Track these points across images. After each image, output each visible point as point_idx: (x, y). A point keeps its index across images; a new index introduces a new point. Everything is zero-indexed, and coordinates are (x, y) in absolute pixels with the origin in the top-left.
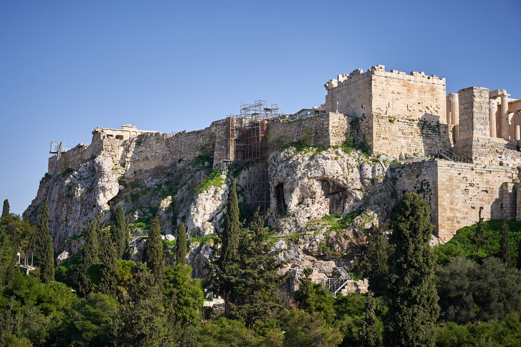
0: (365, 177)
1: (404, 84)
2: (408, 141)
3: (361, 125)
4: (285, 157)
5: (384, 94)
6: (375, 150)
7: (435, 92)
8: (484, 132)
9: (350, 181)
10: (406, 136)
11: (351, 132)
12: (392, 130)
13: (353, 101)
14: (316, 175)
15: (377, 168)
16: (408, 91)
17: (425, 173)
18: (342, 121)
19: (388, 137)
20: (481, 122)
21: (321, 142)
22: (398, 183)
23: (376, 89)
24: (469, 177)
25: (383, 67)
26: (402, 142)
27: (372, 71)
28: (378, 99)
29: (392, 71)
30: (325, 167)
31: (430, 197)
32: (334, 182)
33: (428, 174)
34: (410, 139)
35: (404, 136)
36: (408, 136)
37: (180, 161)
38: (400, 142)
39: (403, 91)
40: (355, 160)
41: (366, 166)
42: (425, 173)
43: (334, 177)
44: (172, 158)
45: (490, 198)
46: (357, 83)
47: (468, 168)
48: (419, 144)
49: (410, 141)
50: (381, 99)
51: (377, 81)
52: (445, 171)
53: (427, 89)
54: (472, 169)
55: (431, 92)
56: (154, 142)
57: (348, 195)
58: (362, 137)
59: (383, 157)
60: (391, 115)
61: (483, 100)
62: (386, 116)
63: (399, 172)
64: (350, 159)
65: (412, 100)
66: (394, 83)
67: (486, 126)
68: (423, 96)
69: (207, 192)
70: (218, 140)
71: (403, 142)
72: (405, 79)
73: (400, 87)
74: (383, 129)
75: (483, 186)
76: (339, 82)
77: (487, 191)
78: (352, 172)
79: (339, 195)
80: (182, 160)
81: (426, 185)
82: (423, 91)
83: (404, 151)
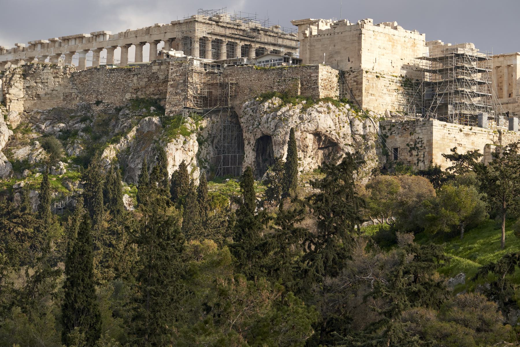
0: (356, 133)
3: (348, 79)
4: (269, 108)
6: (364, 106)
7: (416, 48)
9: (343, 136)
12: (379, 86)
13: (338, 53)
14: (309, 128)
15: (368, 123)
16: (393, 46)
17: (420, 131)
18: (330, 74)
19: (375, 94)
21: (309, 94)
22: (388, 141)
24: (458, 137)
25: (372, 20)
27: (361, 25)
29: (378, 25)
30: (319, 121)
31: (424, 155)
32: (326, 136)
33: (422, 132)
34: (394, 96)
35: (389, 93)
37: (98, 103)
41: (357, 122)
42: (420, 131)
43: (327, 131)
44: (81, 99)
46: (343, 35)
47: (457, 128)
49: (394, 98)
54: (461, 131)
56: (51, 77)
57: (339, 150)
58: (349, 92)
59: (371, 113)
60: (378, 71)
62: (373, 71)
63: (390, 130)
64: (341, 113)
69: (177, 141)
70: (172, 82)
72: (391, 34)
74: (371, 85)
76: (319, 31)
78: (344, 127)
79: (329, 150)
80: (101, 102)
81: (420, 143)
82: (405, 46)
83: (389, 109)
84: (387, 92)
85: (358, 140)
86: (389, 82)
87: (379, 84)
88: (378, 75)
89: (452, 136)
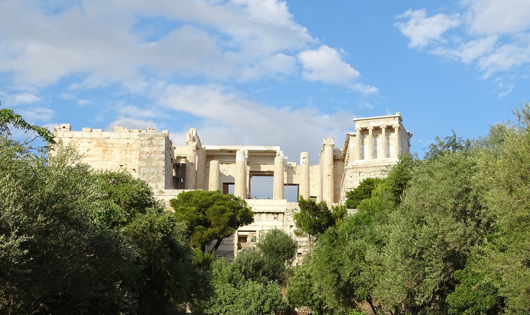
1: (99, 143)
16: (104, 152)
61: (154, 149)
67: (158, 184)
68: (128, 156)
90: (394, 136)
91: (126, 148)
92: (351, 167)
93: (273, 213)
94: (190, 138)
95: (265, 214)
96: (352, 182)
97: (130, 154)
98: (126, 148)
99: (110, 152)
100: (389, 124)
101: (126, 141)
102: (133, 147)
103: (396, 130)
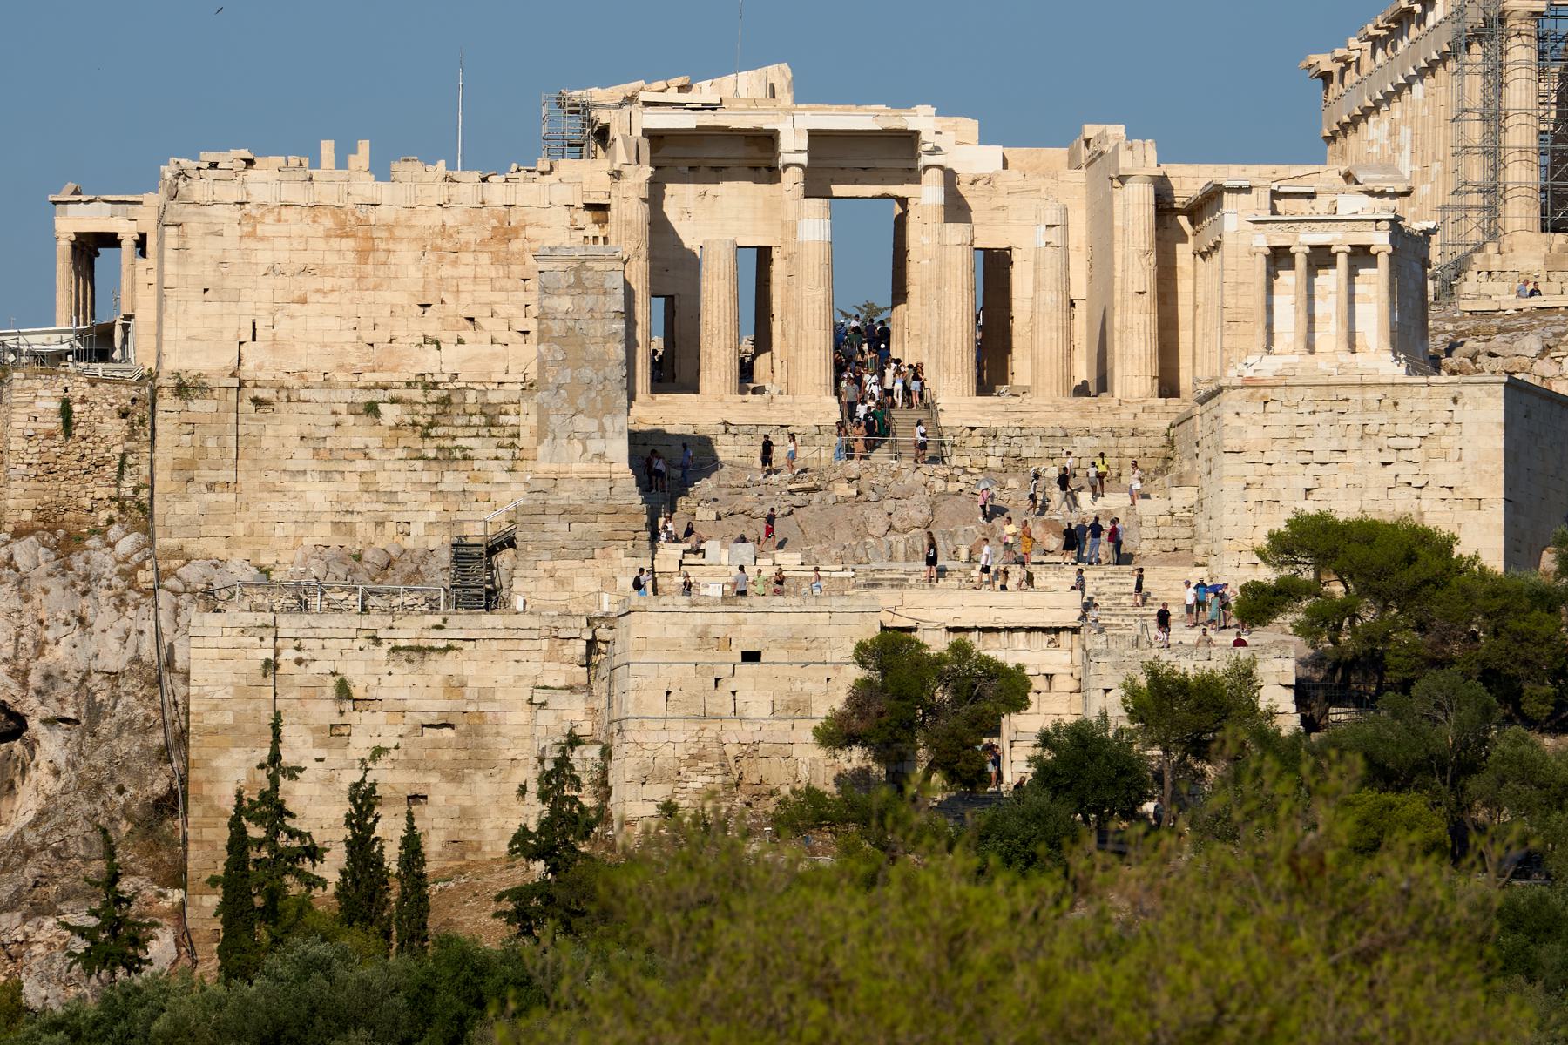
1: (342, 224)
2: (343, 487)
5: (230, 283)
6: (162, 542)
7: (515, 246)
8: (595, 446)
10: (332, 466)
11: (123, 456)
12: (265, 444)
16: (363, 255)
20: (581, 403)
23: (180, 263)
26: (310, 496)
28: (197, 307)
36: (347, 467)
38: (299, 497)
39: (332, 259)
40: (81, 586)
45: (463, 755)
47: (352, 633)
48: (400, 497)
49: (352, 485)
50: (214, 307)
51: (194, 225)
52: (226, 653)
53: (468, 235)
55: (494, 246)
60: (263, 376)
61: (589, 301)
64: (55, 585)
65: (386, 296)
66: (282, 229)
67: (607, 421)
68: (446, 271)
71: (317, 493)
73: (321, 244)
75: (427, 705)
77: (452, 726)
78: (57, 642)
82: (447, 245)
84: (313, 464)
85: (99, 697)
86: (333, 419)
87: (269, 432)
88: (261, 394)
89: (323, 666)
90: (1374, 284)
91: (439, 241)
92: (1238, 382)
93: (1045, 630)
94: (628, 153)
95: (1022, 635)
96: (1240, 431)
97: (455, 263)
98: (439, 241)
99: (382, 256)
100: (1361, 239)
101: (437, 216)
102: (463, 238)
103: (1383, 260)
